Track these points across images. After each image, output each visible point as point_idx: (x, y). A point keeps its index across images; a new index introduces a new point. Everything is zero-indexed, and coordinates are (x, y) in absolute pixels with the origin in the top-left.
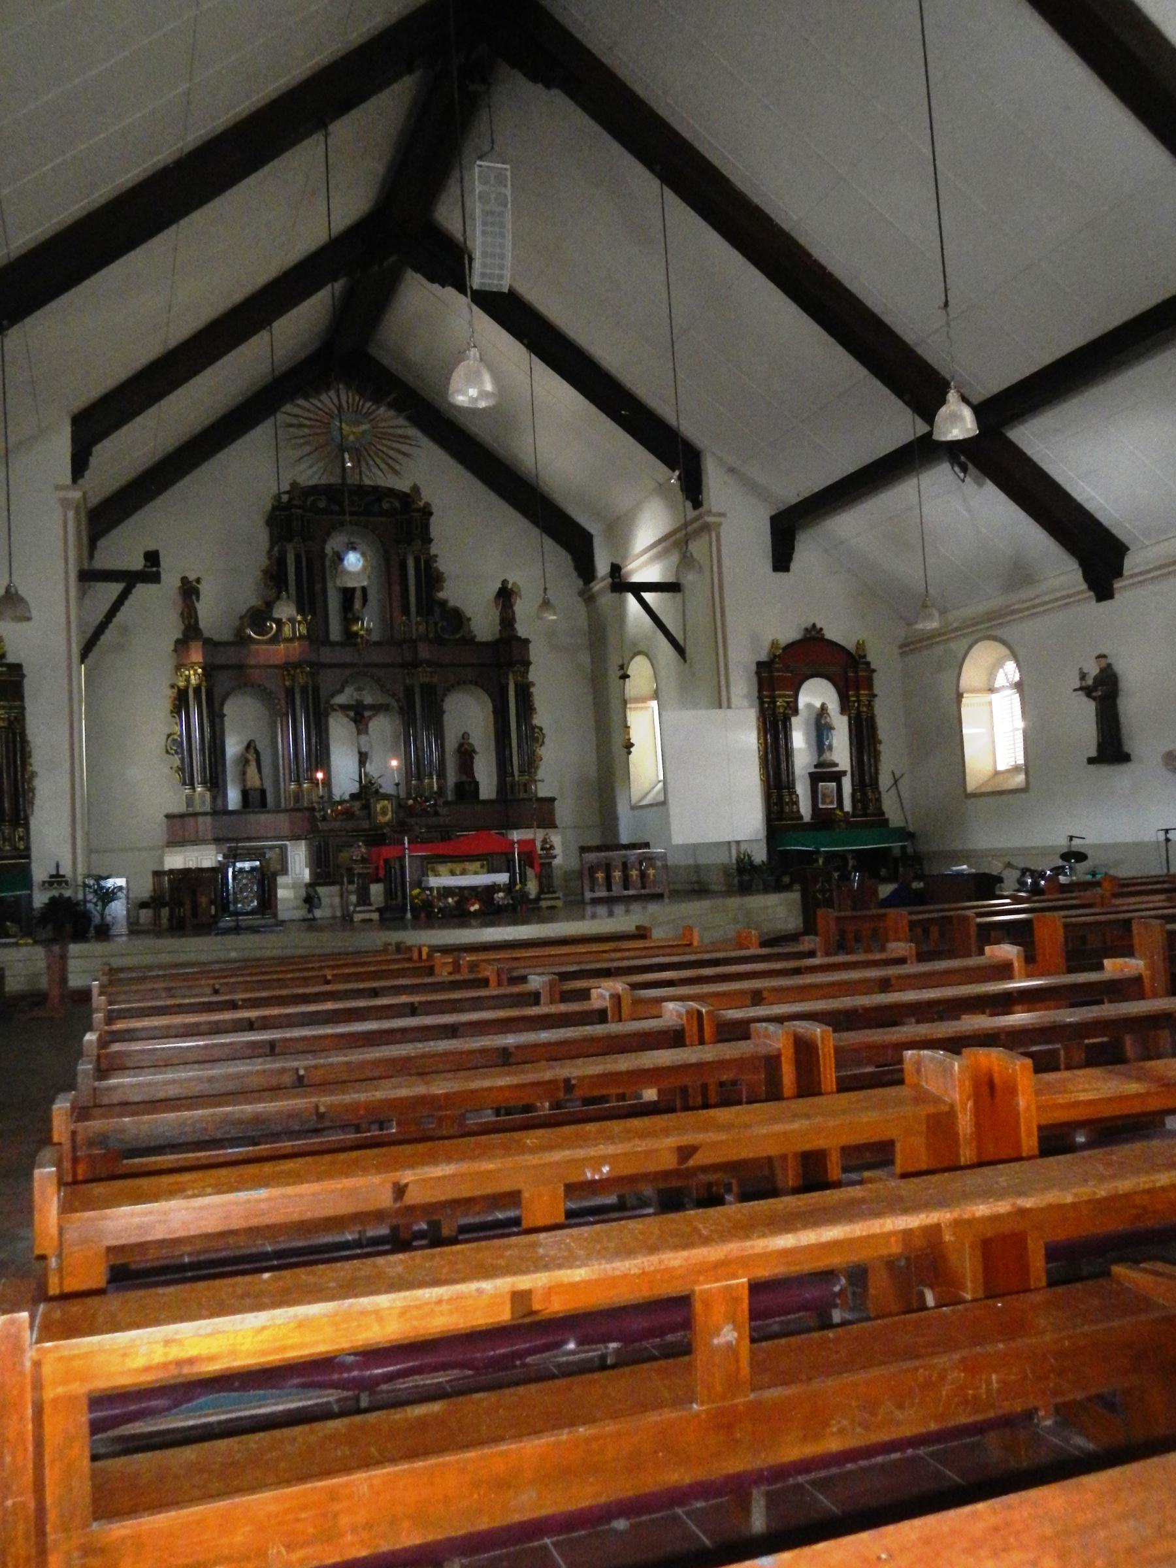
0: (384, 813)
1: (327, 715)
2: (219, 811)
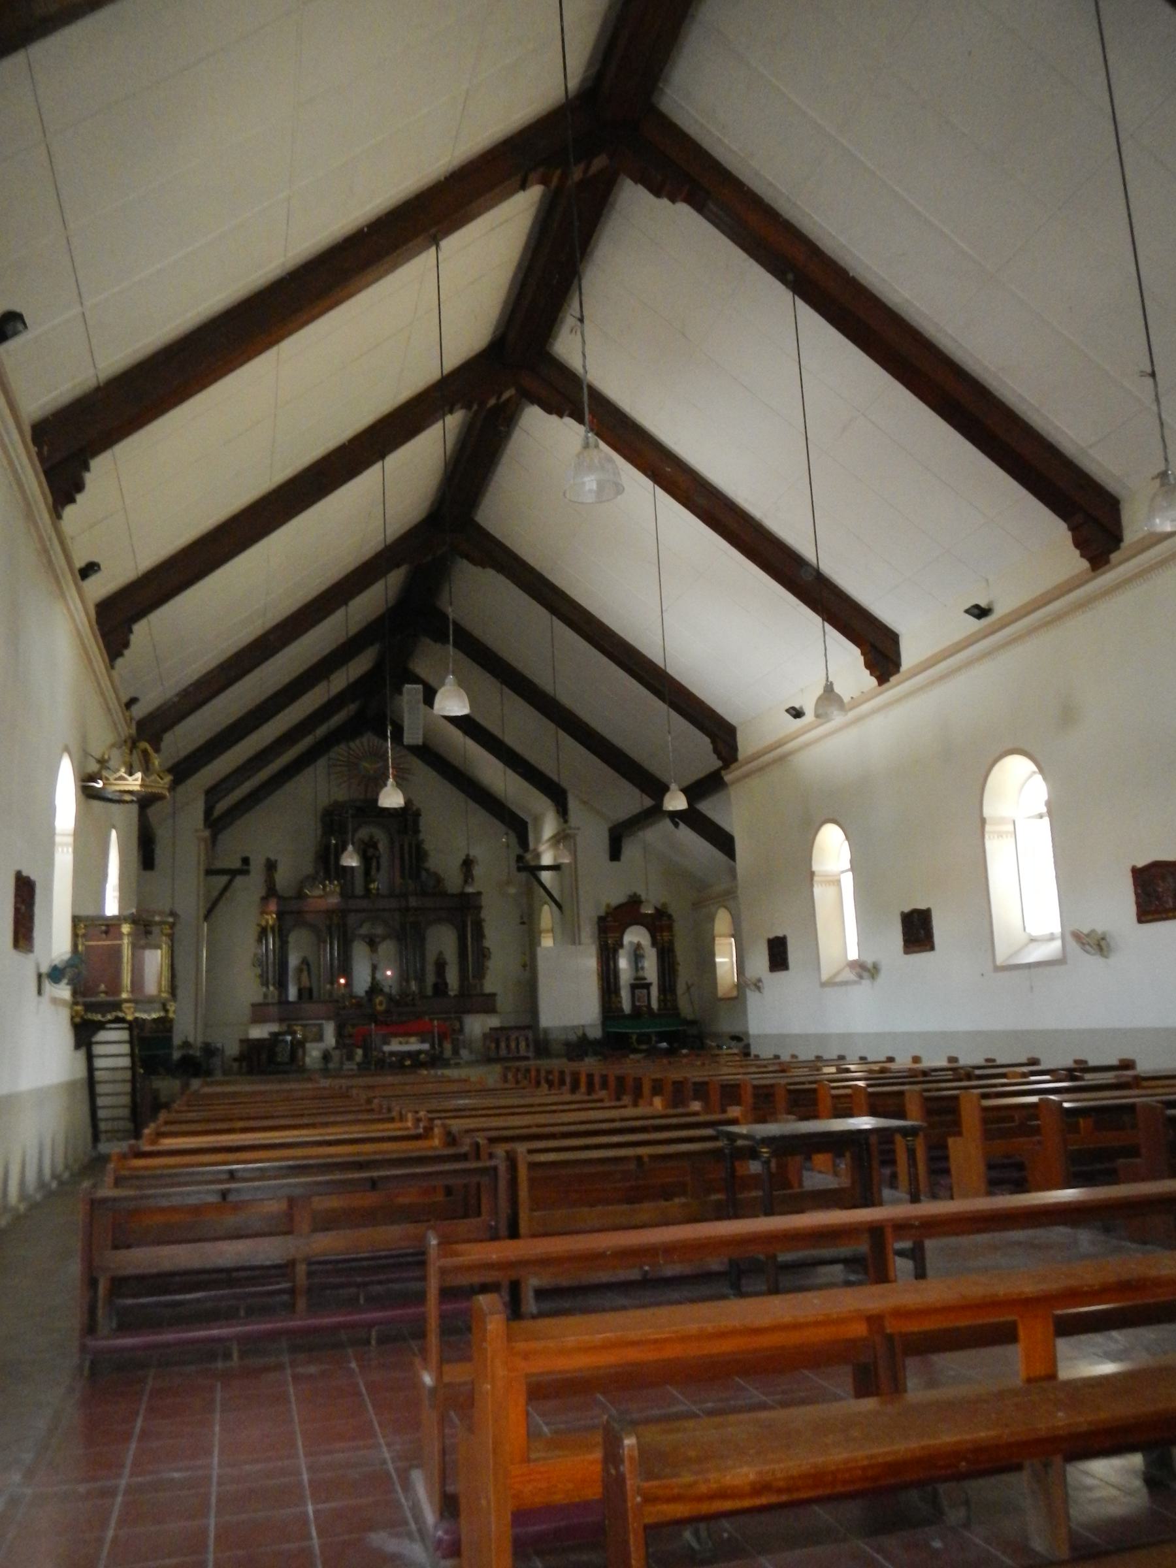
0: (380, 1003)
1: (352, 941)
2: (283, 1002)
